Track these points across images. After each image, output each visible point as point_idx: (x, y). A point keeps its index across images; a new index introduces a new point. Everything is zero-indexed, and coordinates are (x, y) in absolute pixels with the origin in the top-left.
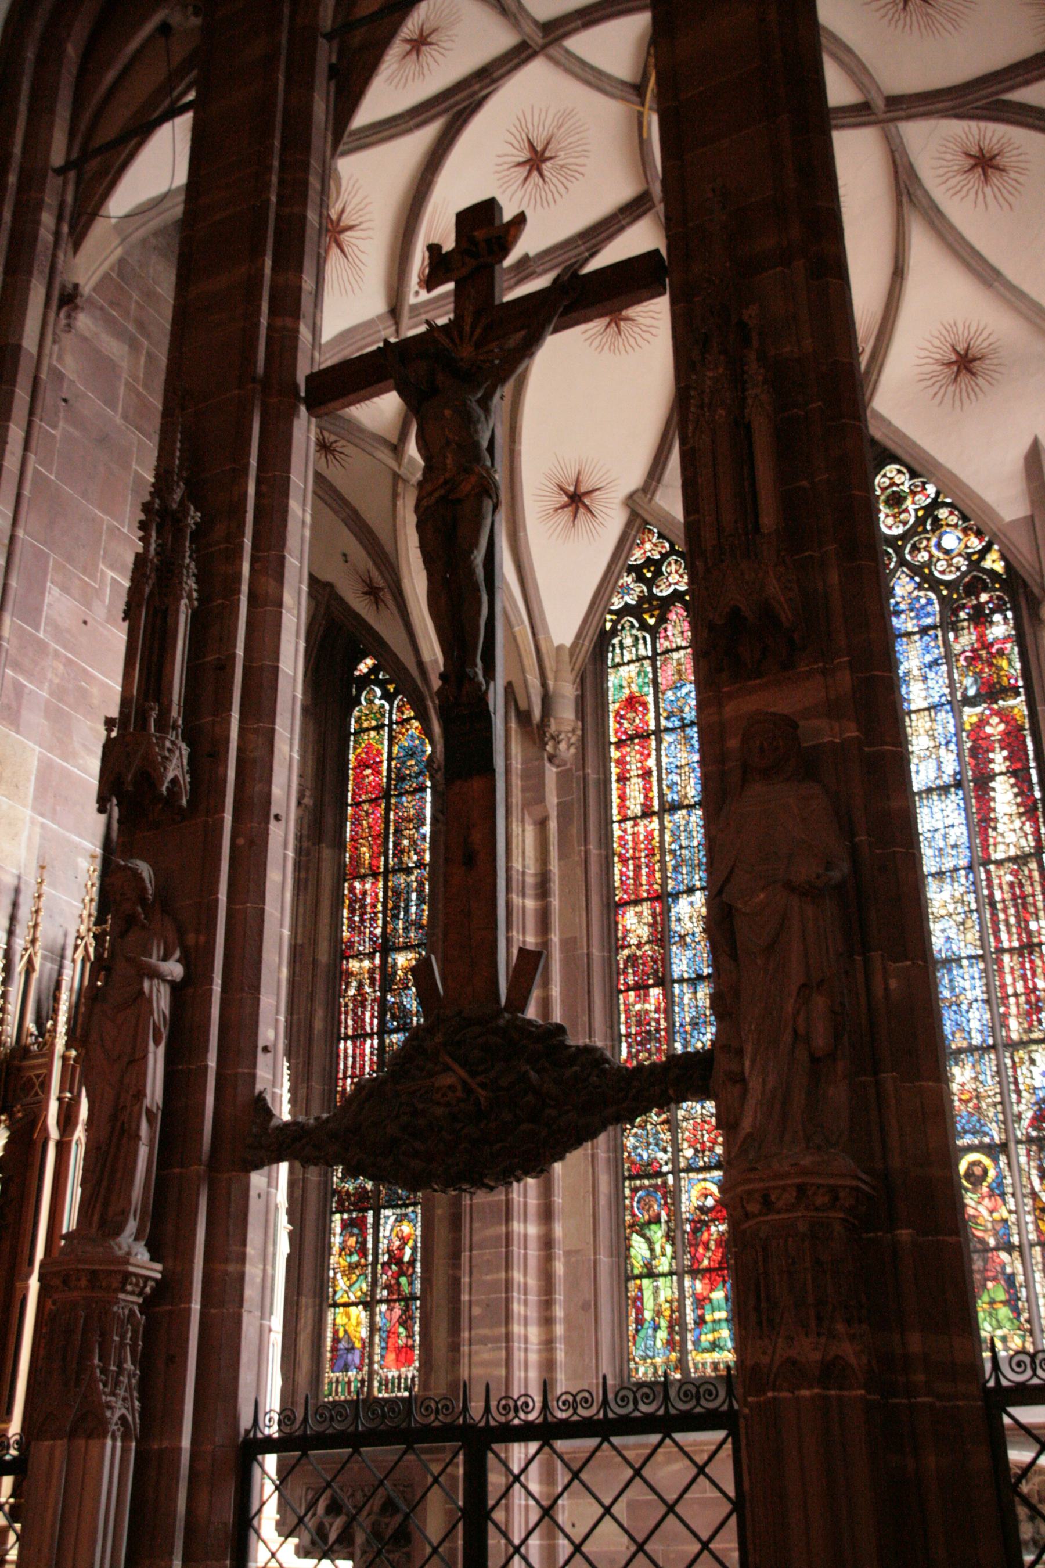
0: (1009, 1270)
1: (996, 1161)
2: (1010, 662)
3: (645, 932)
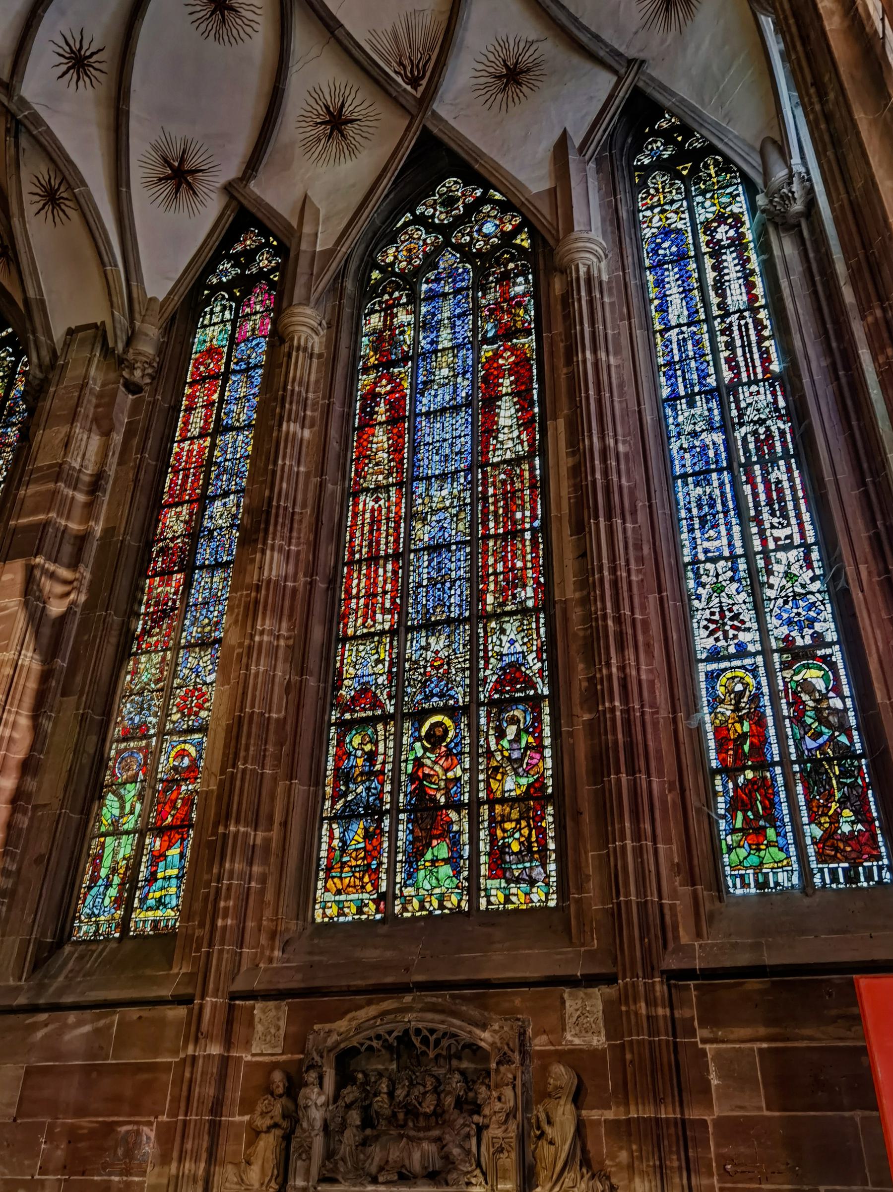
0: (455, 828)
2: (526, 311)
3: (180, 528)
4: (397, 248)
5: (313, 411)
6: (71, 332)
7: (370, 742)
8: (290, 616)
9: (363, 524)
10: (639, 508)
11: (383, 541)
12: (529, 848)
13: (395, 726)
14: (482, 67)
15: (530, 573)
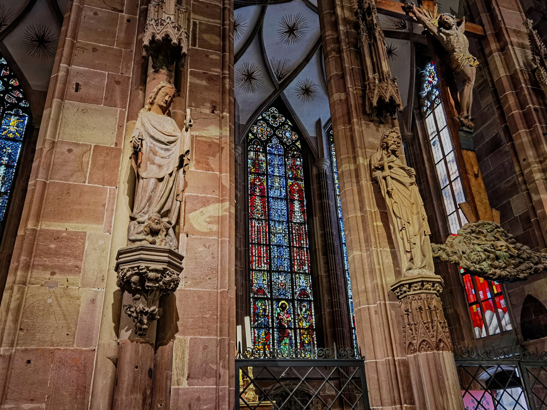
0: (290, 335)
1: (289, 304)
4: (257, 128)
7: (264, 305)
9: (255, 231)
11: (262, 239)
12: (310, 343)
13: (271, 302)
14: (299, 84)
15: (306, 262)
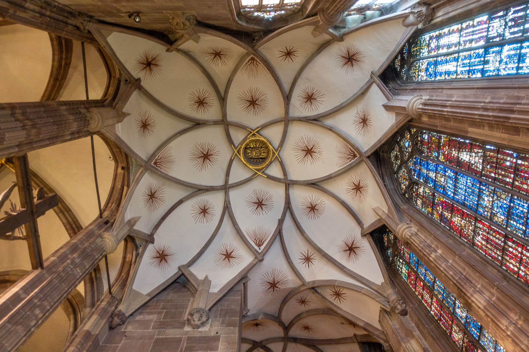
2: (434, 136)
3: (461, 336)
5: (433, 244)
6: (380, 321)
8: (509, 309)
10: (518, 95)
11: (497, 241)
